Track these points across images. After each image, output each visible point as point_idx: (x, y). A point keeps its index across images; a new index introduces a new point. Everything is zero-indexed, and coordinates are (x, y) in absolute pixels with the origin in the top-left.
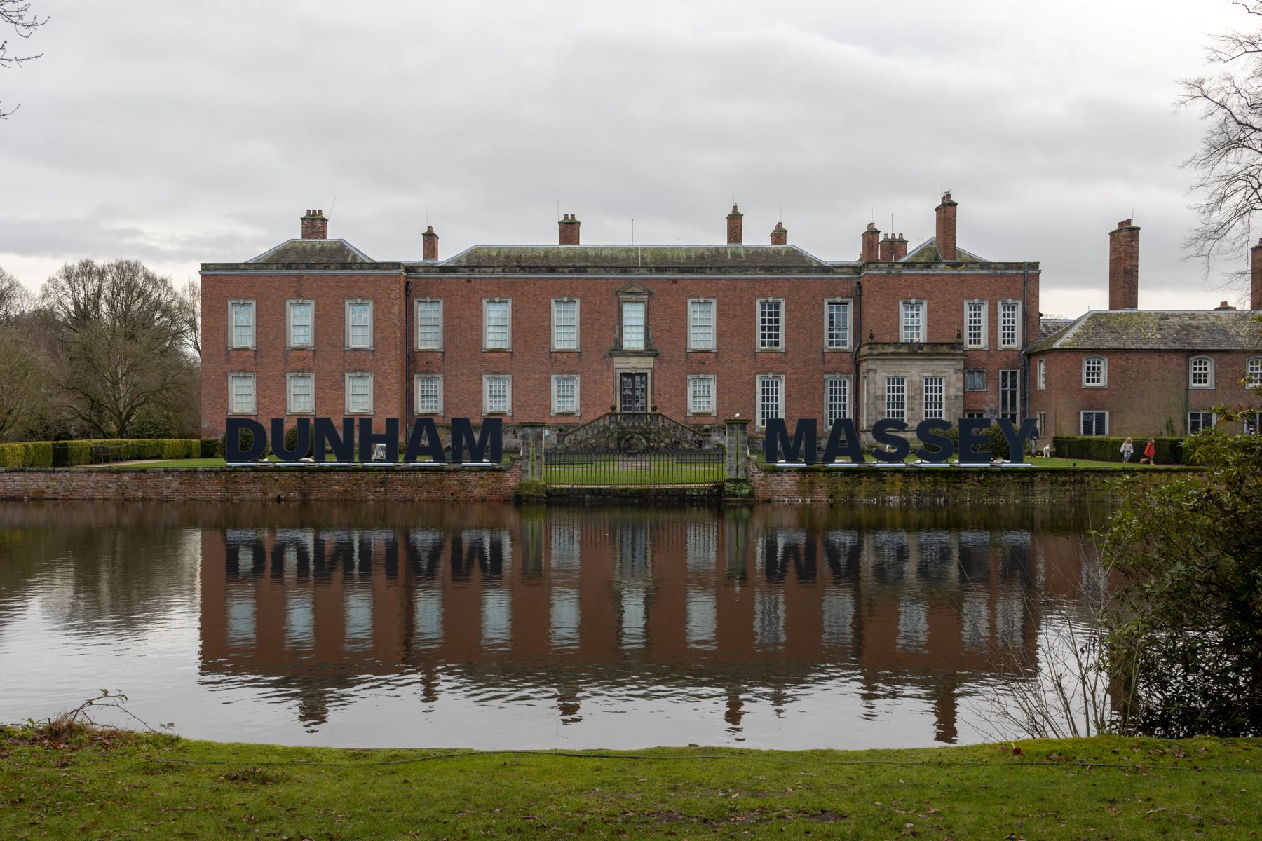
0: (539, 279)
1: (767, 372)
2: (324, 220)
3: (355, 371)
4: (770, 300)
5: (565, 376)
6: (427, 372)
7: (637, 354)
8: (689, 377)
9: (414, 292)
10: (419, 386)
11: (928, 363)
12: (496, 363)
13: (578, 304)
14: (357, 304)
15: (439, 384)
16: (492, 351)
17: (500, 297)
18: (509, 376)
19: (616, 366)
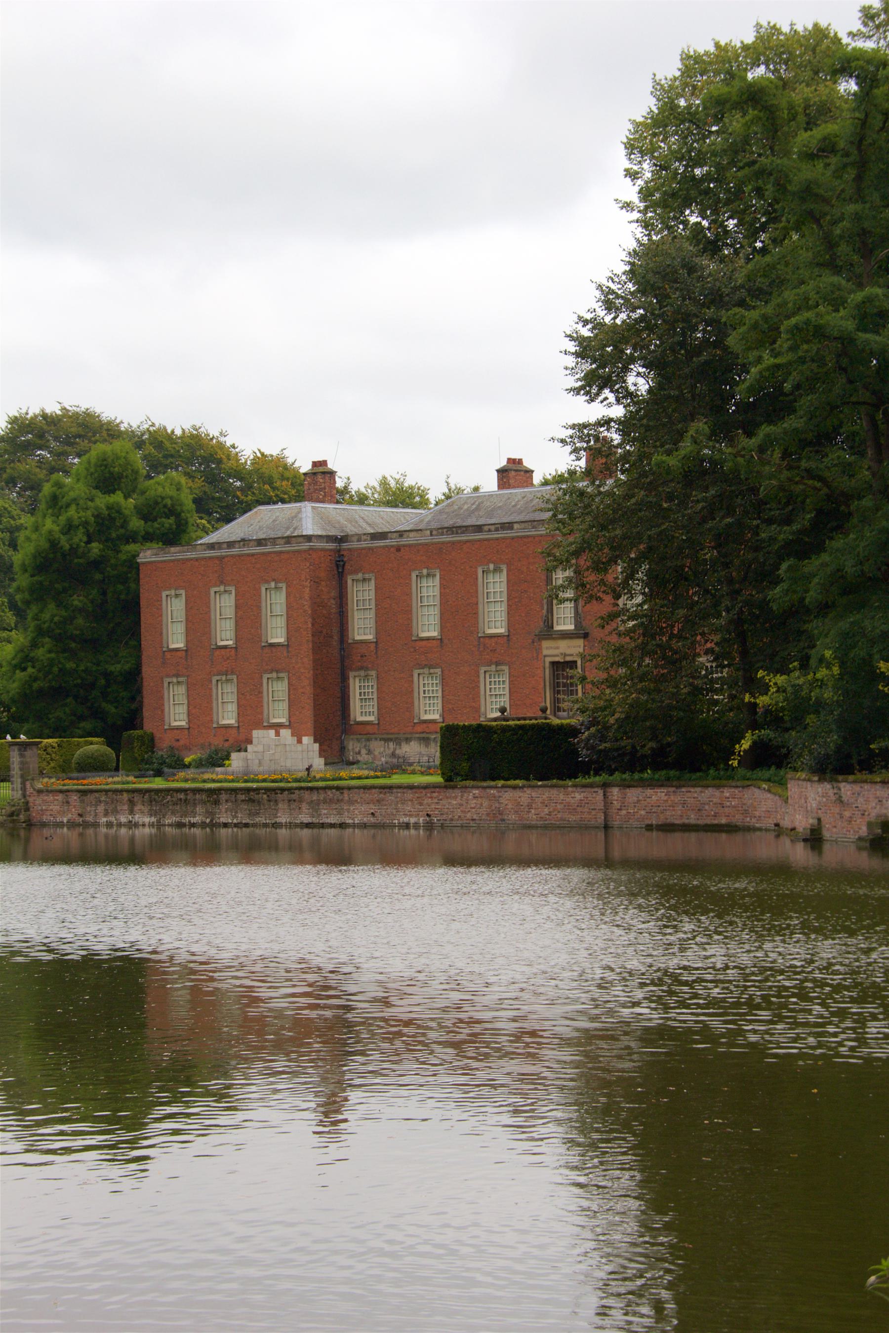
0: (467, 541)
2: (332, 474)
7: (565, 635)
9: (347, 567)
10: (356, 686)
12: (426, 655)
13: (505, 572)
15: (373, 683)
16: (422, 639)
18: (439, 671)
19: (545, 652)
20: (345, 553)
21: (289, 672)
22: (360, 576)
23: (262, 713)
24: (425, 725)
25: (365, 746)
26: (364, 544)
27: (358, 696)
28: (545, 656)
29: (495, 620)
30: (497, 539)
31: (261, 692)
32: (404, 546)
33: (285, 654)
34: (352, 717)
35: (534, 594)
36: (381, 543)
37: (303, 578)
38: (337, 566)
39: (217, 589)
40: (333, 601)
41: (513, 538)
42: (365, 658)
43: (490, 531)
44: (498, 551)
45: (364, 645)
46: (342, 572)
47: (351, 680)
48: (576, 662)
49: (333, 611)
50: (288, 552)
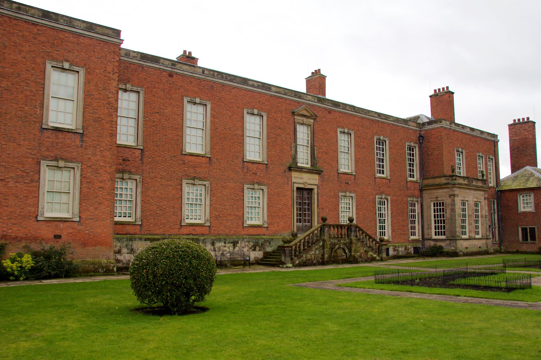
0: (235, 88)
1: (381, 193)
3: (56, 160)
4: (382, 138)
5: (256, 186)
8: (340, 194)
11: (475, 192)
12: (195, 168)
14: (63, 69)
16: (191, 155)
17: (201, 99)
18: (207, 183)
19: (294, 180)
21: (82, 163)
25: (127, 245)
29: (254, 151)
30: (259, 93)
33: (78, 143)
35: (286, 138)
37: (109, 69)
42: (128, 162)
44: (259, 102)
45: (127, 150)
48: (311, 190)
50: (91, 38)
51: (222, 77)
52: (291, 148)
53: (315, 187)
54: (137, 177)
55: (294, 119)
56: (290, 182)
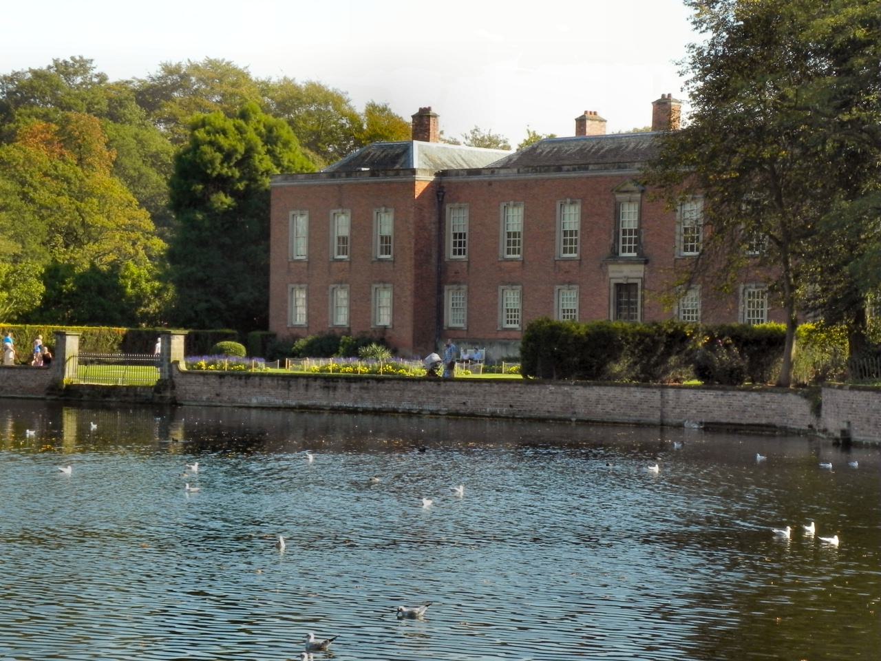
6: (454, 283)
9: (447, 197)
19: (611, 275)
20: (445, 185)
22: (457, 205)
23: (369, 317)
24: (506, 333)
26: (461, 179)
27: (451, 306)
28: (610, 278)
30: (574, 178)
31: (369, 300)
32: (495, 181)
33: (392, 269)
34: (445, 324)
36: (476, 178)
38: (438, 195)
39: (335, 211)
40: (433, 226)
41: (588, 178)
43: (568, 170)
46: (442, 201)
47: (446, 294)
48: (636, 284)
49: (433, 233)
51: (536, 171)
52: (610, 236)
53: (639, 281)
54: (464, 287)
55: (615, 199)
56: (607, 278)
